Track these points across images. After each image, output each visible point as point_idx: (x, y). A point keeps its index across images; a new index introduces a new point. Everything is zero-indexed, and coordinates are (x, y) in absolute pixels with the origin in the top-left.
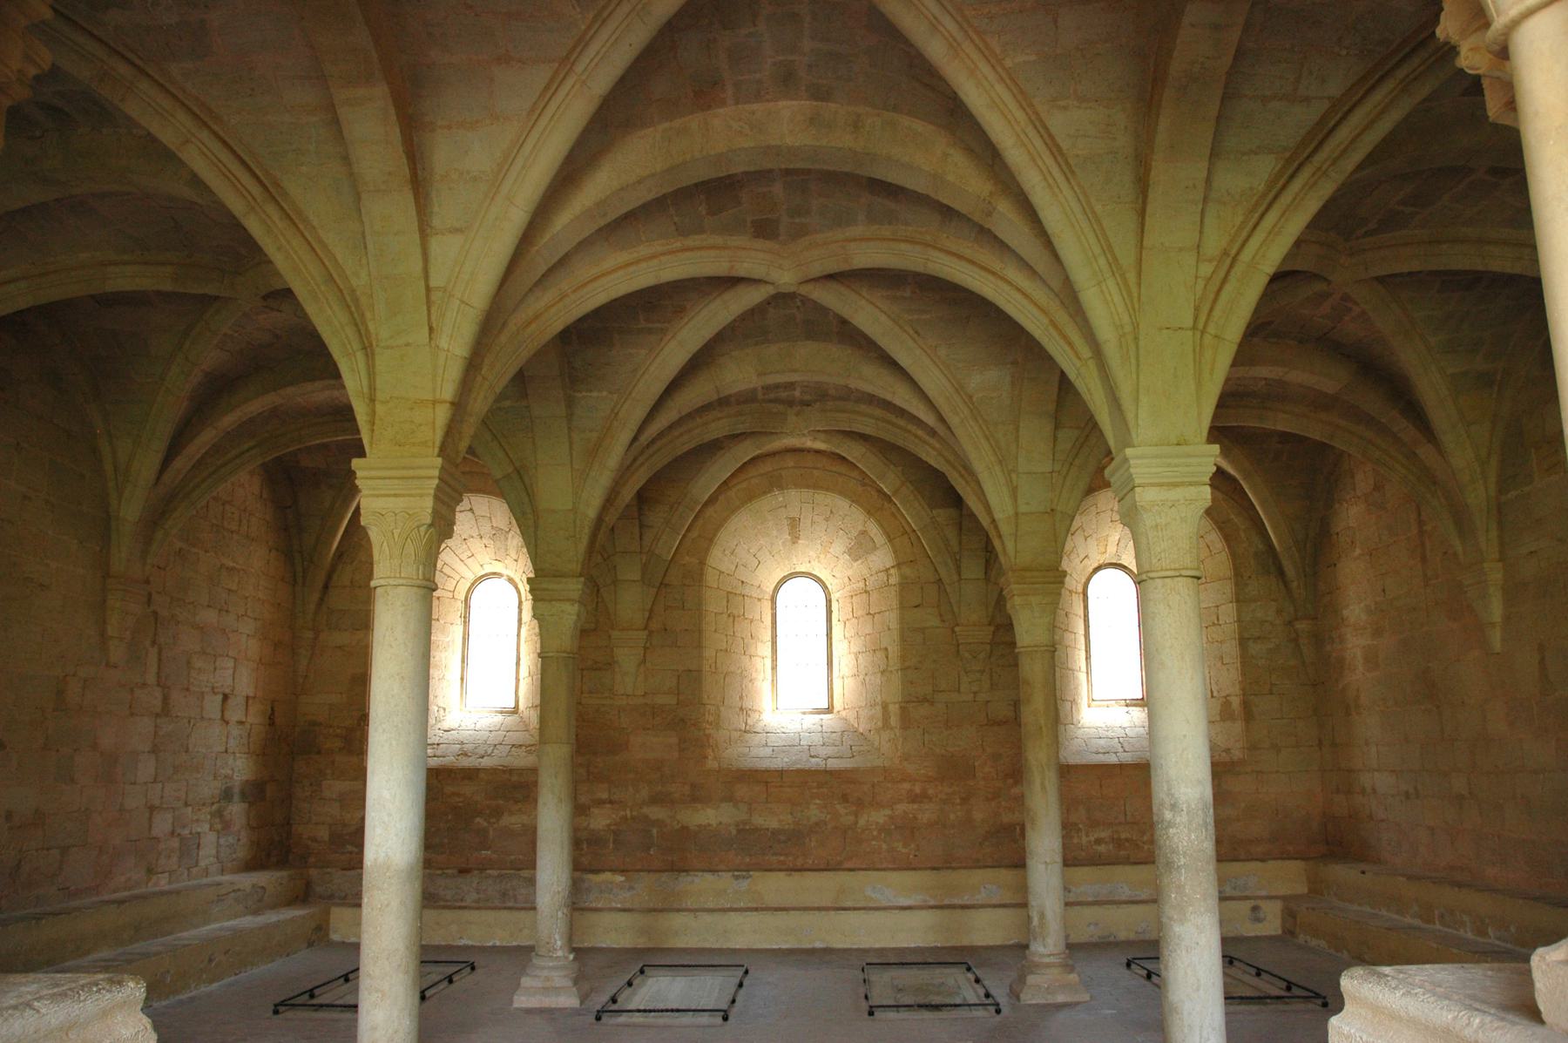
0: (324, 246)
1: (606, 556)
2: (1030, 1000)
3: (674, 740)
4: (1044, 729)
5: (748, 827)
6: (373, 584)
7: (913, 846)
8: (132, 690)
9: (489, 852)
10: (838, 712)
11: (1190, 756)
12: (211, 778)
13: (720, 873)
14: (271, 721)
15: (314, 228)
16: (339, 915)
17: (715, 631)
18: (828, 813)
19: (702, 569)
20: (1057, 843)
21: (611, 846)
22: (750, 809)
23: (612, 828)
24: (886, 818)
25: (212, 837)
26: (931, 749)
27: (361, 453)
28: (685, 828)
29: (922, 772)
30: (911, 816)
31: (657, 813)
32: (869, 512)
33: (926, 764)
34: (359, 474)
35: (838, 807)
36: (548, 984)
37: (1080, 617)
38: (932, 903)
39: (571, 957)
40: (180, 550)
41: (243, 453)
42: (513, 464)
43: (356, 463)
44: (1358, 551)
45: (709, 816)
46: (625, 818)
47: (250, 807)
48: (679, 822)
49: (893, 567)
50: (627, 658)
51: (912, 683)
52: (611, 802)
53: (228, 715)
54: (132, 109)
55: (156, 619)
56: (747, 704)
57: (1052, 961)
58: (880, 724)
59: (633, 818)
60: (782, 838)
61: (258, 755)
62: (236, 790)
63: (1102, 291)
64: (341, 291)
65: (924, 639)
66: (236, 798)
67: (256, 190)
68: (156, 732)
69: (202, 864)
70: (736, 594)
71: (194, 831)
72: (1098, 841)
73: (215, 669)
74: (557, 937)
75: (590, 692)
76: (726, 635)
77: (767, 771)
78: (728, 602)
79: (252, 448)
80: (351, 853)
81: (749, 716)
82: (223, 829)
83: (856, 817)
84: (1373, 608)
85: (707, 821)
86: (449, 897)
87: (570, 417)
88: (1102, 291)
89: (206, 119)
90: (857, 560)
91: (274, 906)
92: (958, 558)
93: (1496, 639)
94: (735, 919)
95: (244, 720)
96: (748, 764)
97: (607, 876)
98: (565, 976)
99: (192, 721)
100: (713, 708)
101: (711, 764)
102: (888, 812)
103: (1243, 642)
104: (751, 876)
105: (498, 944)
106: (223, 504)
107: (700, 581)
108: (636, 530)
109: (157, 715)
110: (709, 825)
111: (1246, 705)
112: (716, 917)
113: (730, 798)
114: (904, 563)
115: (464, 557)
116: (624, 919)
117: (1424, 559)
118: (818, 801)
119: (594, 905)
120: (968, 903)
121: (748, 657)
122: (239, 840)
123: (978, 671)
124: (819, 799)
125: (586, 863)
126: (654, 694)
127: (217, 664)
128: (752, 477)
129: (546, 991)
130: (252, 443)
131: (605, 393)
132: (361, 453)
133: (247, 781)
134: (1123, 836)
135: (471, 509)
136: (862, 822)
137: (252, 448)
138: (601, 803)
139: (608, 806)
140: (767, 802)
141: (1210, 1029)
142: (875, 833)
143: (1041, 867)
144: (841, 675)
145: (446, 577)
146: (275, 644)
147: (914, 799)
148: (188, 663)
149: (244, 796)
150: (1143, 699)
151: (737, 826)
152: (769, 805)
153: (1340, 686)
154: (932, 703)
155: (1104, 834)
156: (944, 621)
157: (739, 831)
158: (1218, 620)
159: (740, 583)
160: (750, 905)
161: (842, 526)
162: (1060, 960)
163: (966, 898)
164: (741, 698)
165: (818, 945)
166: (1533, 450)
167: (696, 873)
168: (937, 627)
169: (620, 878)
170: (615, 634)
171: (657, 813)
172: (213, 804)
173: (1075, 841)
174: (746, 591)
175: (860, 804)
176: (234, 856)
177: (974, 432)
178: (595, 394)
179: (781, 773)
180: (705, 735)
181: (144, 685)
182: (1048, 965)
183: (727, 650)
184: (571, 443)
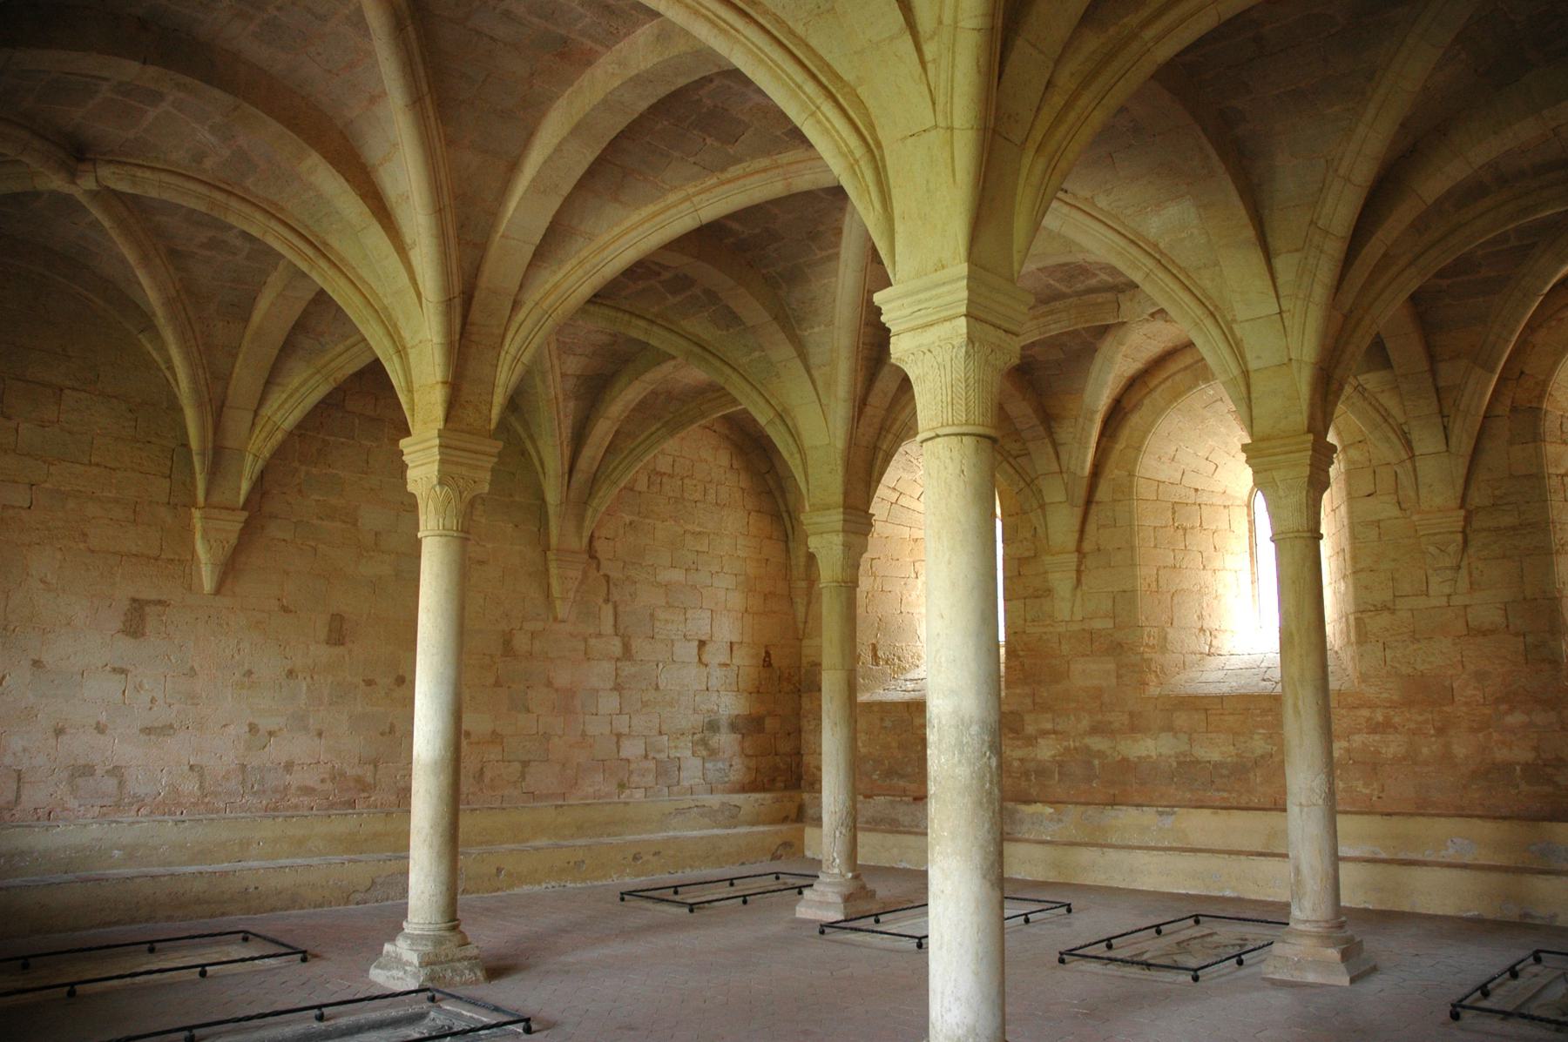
0: (360, 278)
1: (1028, 480)
2: (1272, 973)
3: (1111, 666)
6: (419, 535)
7: (1375, 786)
8: (586, 640)
11: (943, 659)
12: (691, 712)
13: (1144, 808)
14: (767, 662)
15: (354, 268)
16: (809, 832)
17: (1155, 546)
18: (1275, 745)
19: (1131, 482)
20: (1317, 781)
21: (1057, 776)
22: (1190, 739)
23: (1057, 758)
24: (1342, 752)
25: (697, 762)
26: (1393, 667)
27: (408, 433)
28: (1125, 760)
29: (1385, 695)
30: (1372, 749)
31: (1097, 743)
34: (405, 451)
36: (822, 899)
38: (1384, 855)
39: (850, 875)
40: (631, 523)
41: (652, 434)
42: (775, 409)
43: (403, 443)
45: (1149, 747)
46: (1067, 749)
47: (743, 737)
48: (1119, 754)
50: (1062, 582)
51: (1366, 588)
52: (1055, 732)
53: (705, 658)
54: (232, 220)
55: (608, 582)
56: (1210, 623)
57: (1308, 929)
59: (1076, 749)
60: (1225, 772)
61: (750, 693)
62: (724, 722)
63: (819, 122)
64: (376, 311)
65: (1380, 534)
66: (724, 729)
67: (310, 252)
68: (617, 675)
69: (685, 784)
71: (672, 756)
73: (686, 619)
74: (835, 855)
75: (1033, 621)
76: (1173, 550)
77: (1206, 697)
78: (1174, 513)
79: (658, 429)
81: (1215, 637)
82: (710, 755)
86: (906, 824)
87: (803, 356)
88: (819, 122)
89: (274, 212)
91: (764, 823)
92: (1406, 430)
94: (1141, 858)
95: (728, 662)
96: (1191, 689)
97: (1038, 807)
98: (838, 893)
99: (661, 666)
100: (1154, 631)
101: (1153, 690)
104: (1174, 813)
106: (682, 479)
107: (1131, 492)
108: (1050, 450)
109: (618, 659)
110: (1150, 757)
112: (1123, 854)
113: (1170, 728)
116: (1038, 852)
118: (1261, 731)
119: (1026, 836)
120: (1428, 859)
121: (1210, 572)
122: (731, 766)
123: (1452, 568)
124: (1263, 728)
125: (1035, 794)
126: (1091, 619)
127: (688, 615)
128: (1175, 374)
130: (659, 425)
131: (823, 327)
132: (408, 433)
133: (738, 715)
137: (658, 429)
138: (1044, 733)
139: (1053, 736)
140: (1207, 732)
141: (952, 999)
146: (765, 595)
147: (1375, 728)
148: (652, 615)
149: (733, 727)
151: (1177, 757)
152: (1210, 735)
154: (1393, 611)
157: (1179, 763)
160: (1175, 845)
162: (1320, 930)
163: (1427, 853)
164: (1201, 617)
165: (1228, 893)
168: (1397, 518)
169: (1049, 810)
170: (1048, 559)
171: (1097, 743)
172: (694, 734)
174: (1204, 498)
176: (726, 779)
177: (1167, 285)
178: (816, 330)
179: (1222, 698)
180: (1145, 660)
181: (599, 635)
182: (1302, 934)
183: (1175, 567)
184: (813, 382)
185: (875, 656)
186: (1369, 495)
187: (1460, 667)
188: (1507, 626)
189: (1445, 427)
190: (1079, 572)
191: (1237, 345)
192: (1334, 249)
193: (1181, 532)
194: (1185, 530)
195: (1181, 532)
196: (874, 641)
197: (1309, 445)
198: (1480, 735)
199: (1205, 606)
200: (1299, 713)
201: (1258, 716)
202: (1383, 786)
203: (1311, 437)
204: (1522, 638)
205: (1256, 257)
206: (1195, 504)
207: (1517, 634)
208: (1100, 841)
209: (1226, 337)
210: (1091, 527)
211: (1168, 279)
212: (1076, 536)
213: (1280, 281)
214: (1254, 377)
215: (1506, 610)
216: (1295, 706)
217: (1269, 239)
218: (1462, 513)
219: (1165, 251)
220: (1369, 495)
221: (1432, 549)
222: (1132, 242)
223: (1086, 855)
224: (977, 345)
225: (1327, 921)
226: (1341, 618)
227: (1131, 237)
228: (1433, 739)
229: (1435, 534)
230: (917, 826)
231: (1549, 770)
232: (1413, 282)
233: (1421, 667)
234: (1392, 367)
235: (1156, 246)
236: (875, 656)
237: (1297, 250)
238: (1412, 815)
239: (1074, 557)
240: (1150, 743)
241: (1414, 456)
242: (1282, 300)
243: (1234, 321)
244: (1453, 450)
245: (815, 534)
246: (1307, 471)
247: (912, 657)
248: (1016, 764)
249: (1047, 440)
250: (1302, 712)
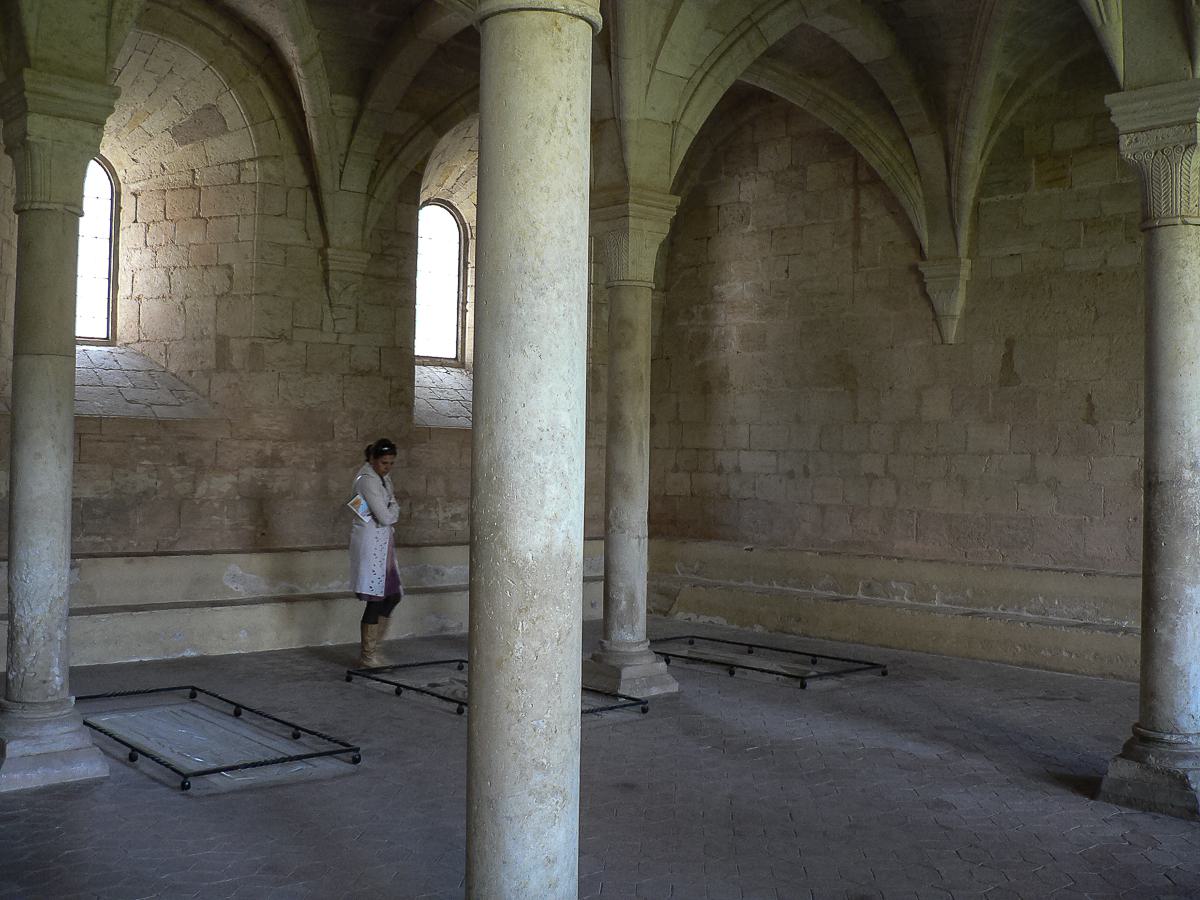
10: (126, 344)
29: (276, 428)
30: (260, 483)
32: (230, 82)
33: (279, 418)
35: (172, 470)
44: (750, 228)
49: (251, 160)
58: (211, 363)
60: (98, 511)
65: (285, 258)
72: (455, 518)
74: (56, 670)
83: (194, 482)
84: (766, 286)
90: (186, 143)
93: (952, 332)
102: (231, 478)
114: (267, 157)
117: (857, 245)
124: (148, 459)
129: (45, 759)
136: (201, 490)
142: (216, 505)
143: (635, 542)
144: (136, 295)
150: (456, 359)
153: (698, 363)
154: (290, 342)
156: (309, 239)
161: (179, 95)
165: (190, 653)
166: (1033, 162)
168: (300, 246)
173: (433, 516)
175: (200, 468)
182: (641, 654)
187: (341, 402)
188: (380, 370)
201: (143, 444)
207: (386, 378)
228: (314, 473)
229: (341, 271)
233: (307, 401)
245: (42, 112)
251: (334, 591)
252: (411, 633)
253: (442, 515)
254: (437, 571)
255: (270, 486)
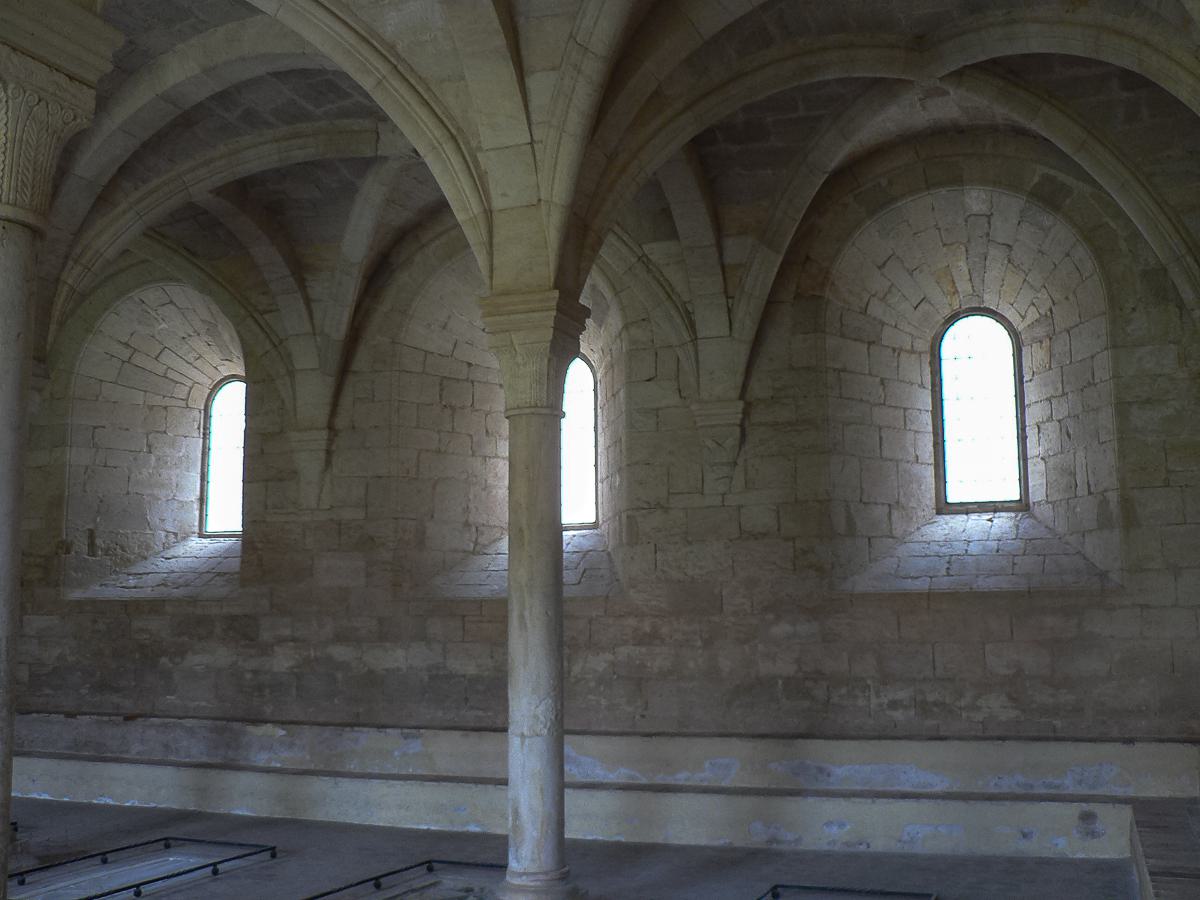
4: (526, 533)
5: (441, 673)
9: (173, 697)
13: (388, 730)
20: (542, 708)
23: (295, 670)
26: (663, 572)
28: (371, 672)
29: (654, 603)
30: (638, 662)
31: (340, 652)
37: (922, 386)
38: (644, 781)
50: (309, 463)
52: (294, 640)
70: (458, 380)
72: (894, 705)
76: (439, 432)
80: (47, 695)
85: (396, 665)
94: (378, 789)
97: (268, 729)
102: (609, 657)
103: (1122, 409)
105: (137, 804)
108: (301, 304)
110: (399, 669)
111: (1126, 502)
115: (191, 357)
134: (931, 698)
135: (171, 302)
138: (281, 641)
139: (291, 644)
140: (463, 641)
142: (592, 684)
145: (173, 384)
147: (642, 639)
150: (1020, 500)
154: (666, 510)
155: (903, 695)
158: (1093, 379)
159: (465, 366)
160: (419, 772)
162: (539, 883)
164: (467, 510)
165: (473, 828)
167: (361, 728)
168: (676, 407)
171: (340, 652)
173: (861, 702)
179: (480, 603)
185: (92, 545)
186: (648, 380)
189: (729, 311)
190: (329, 453)
191: (480, 178)
192: (593, 69)
193: (448, 412)
194: (453, 409)
195: (448, 412)
196: (91, 526)
197: (554, 304)
198: (746, 647)
199: (471, 497)
200: (526, 627)
202: (647, 703)
203: (556, 293)
204: (791, 544)
205: (508, 71)
206: (467, 380)
207: (787, 539)
208: (338, 769)
209: (469, 167)
210: (346, 400)
211: (403, 89)
212: (327, 410)
213: (534, 103)
214: (498, 219)
215: (778, 512)
216: (522, 617)
217: (524, 53)
218: (741, 405)
219: (403, 55)
220: (648, 380)
221: (709, 443)
222: (364, 39)
223: (320, 786)
224: (11, 86)
225: (546, 873)
226: (614, 516)
227: (363, 33)
228: (700, 651)
229: (713, 426)
230: (127, 752)
231: (809, 684)
232: (688, 129)
234: (677, 238)
235: (392, 47)
236: (92, 545)
237: (553, 69)
238: (673, 735)
239: (324, 434)
240: (400, 653)
241: (696, 339)
242: (533, 127)
243: (480, 149)
244: (736, 335)
246: (549, 334)
247: (139, 547)
248: (248, 676)
249: (299, 295)
250: (529, 625)
251: (681, 783)
252: (727, 841)
253: (874, 701)
254: (821, 770)
255: (649, 665)
